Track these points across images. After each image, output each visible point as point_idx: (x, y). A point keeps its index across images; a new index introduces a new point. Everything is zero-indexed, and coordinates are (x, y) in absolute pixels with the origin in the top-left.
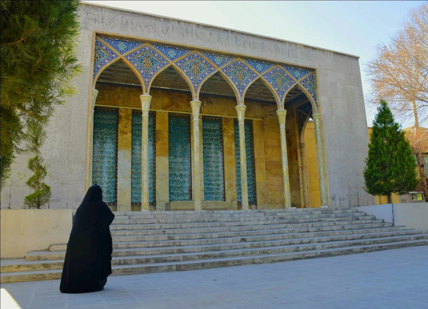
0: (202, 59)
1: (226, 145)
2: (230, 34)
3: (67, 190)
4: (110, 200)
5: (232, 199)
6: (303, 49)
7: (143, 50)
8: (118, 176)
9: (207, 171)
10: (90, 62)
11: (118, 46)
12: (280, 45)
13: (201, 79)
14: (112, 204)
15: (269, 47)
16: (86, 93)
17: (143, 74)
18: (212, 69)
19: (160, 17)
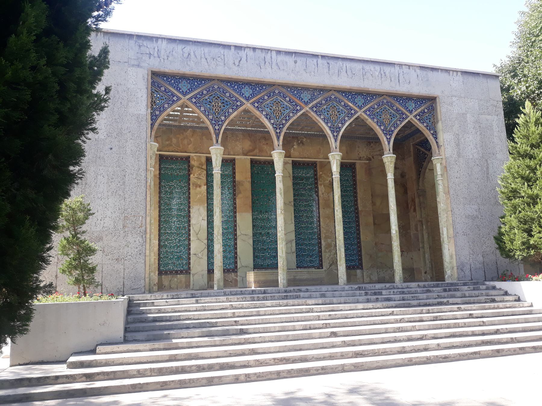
0: (285, 96)
1: (322, 196)
2: (320, 61)
3: (123, 266)
4: (182, 268)
5: (331, 263)
6: (418, 71)
7: (211, 89)
8: (192, 238)
9: (299, 228)
10: (146, 108)
11: (180, 85)
12: (387, 69)
13: (284, 122)
14: (184, 272)
15: (372, 73)
16: (143, 147)
17: (212, 120)
18: (298, 108)
19: (230, 44)
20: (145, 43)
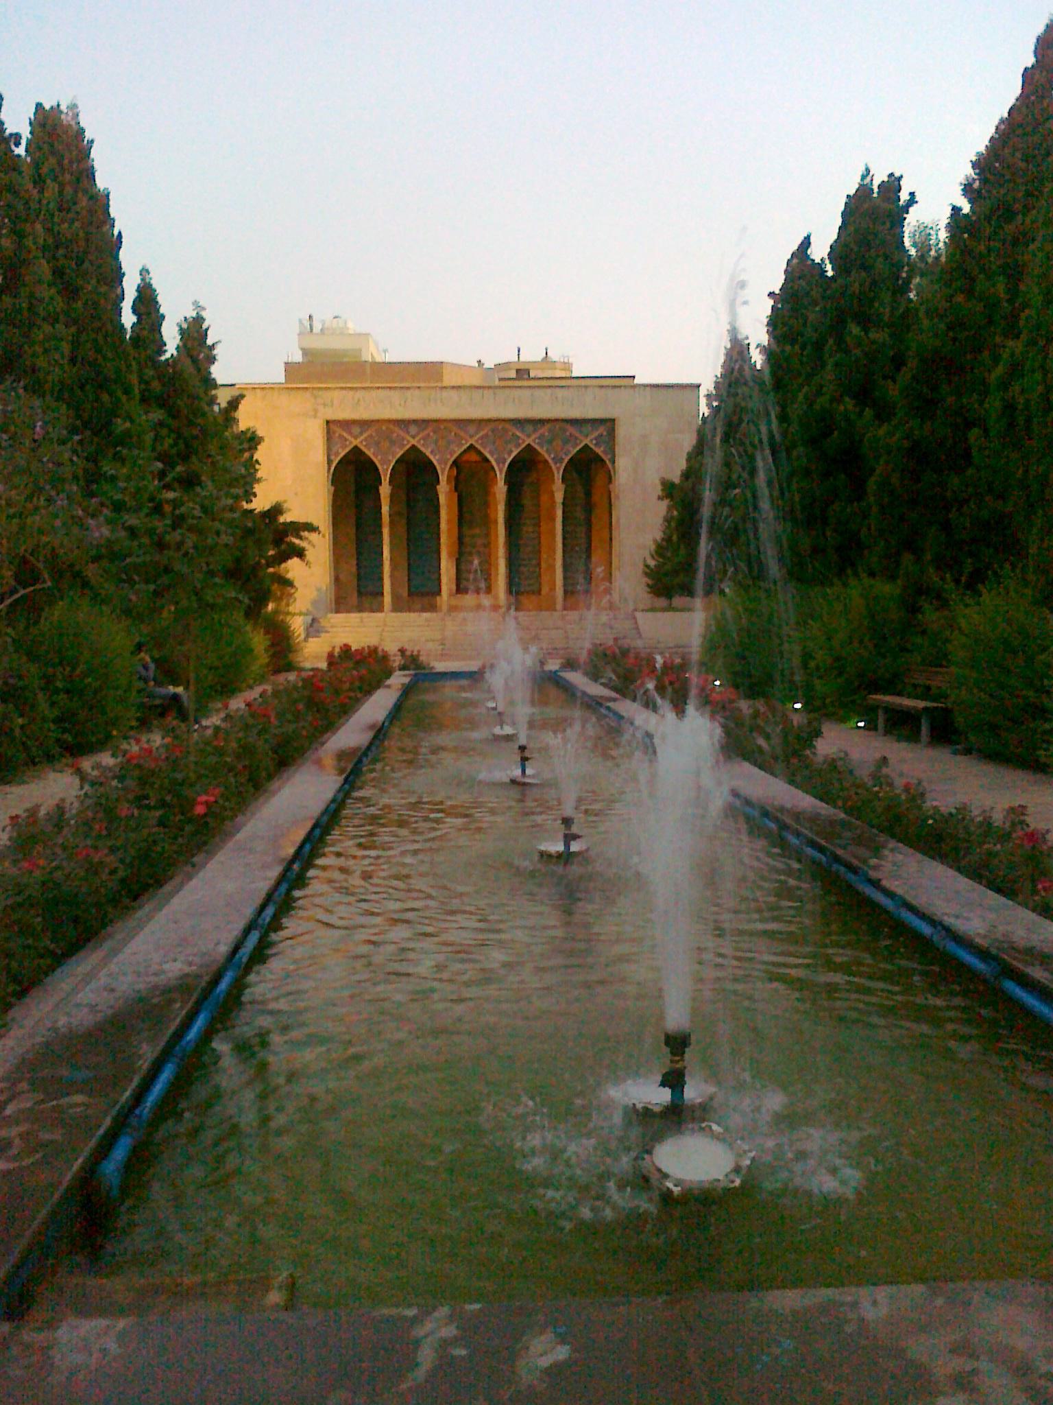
20: (320, 393)
